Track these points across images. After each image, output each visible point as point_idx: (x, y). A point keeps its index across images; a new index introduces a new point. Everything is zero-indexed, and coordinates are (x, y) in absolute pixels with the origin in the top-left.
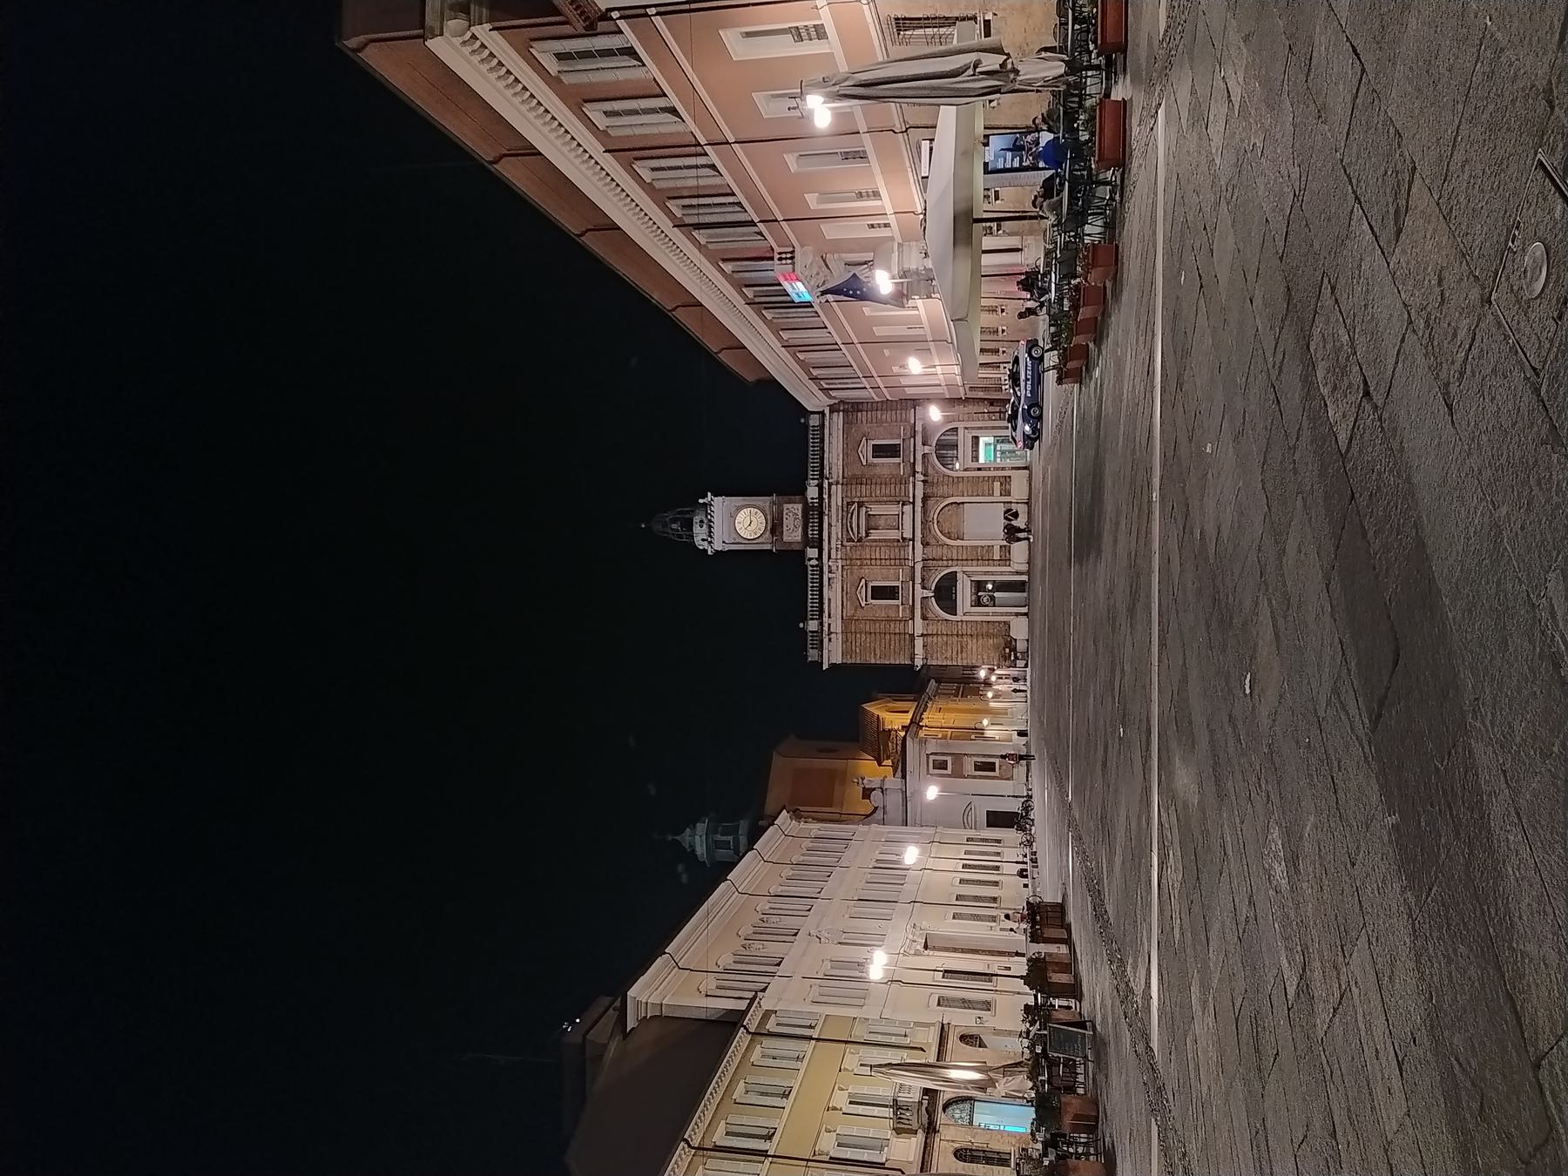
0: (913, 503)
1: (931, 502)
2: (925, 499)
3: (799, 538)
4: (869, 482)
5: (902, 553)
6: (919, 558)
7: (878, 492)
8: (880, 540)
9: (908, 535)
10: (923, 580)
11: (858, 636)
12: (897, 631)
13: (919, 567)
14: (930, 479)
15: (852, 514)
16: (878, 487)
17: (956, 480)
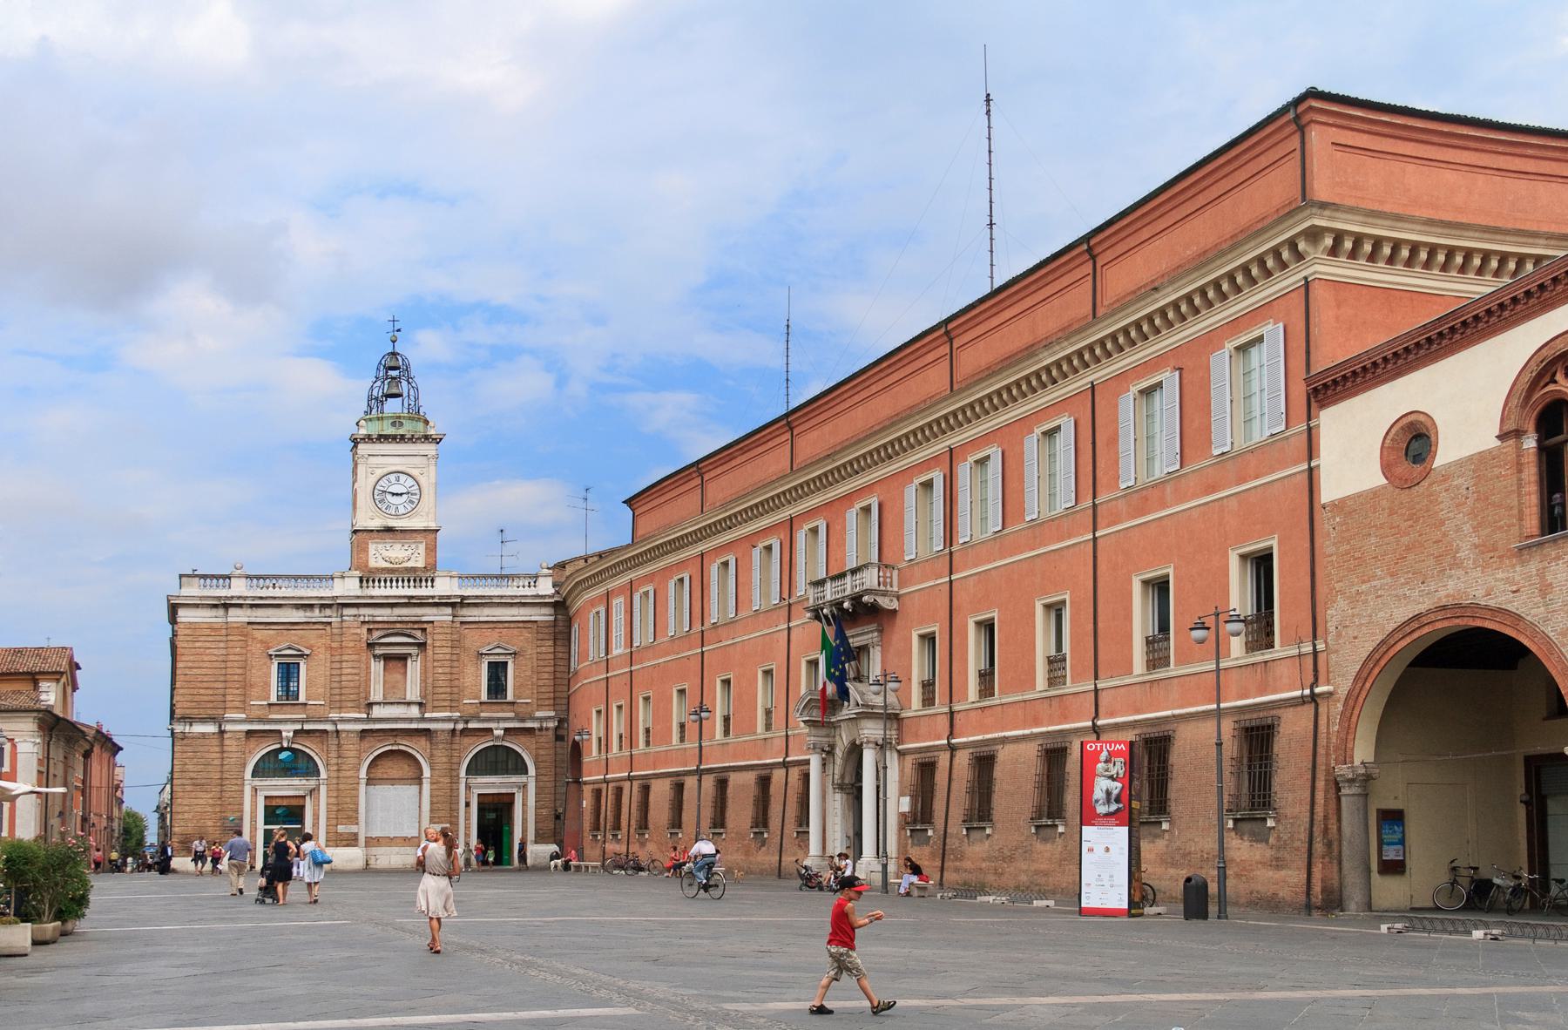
0: (423, 719)
1: (423, 742)
2: (427, 733)
3: (373, 563)
4: (455, 657)
5: (350, 704)
6: (340, 727)
7: (440, 670)
8: (368, 673)
9: (377, 712)
10: (309, 732)
11: (222, 645)
12: (229, 698)
13: (329, 727)
14: (457, 739)
15: (409, 636)
16: (448, 670)
17: (455, 774)
